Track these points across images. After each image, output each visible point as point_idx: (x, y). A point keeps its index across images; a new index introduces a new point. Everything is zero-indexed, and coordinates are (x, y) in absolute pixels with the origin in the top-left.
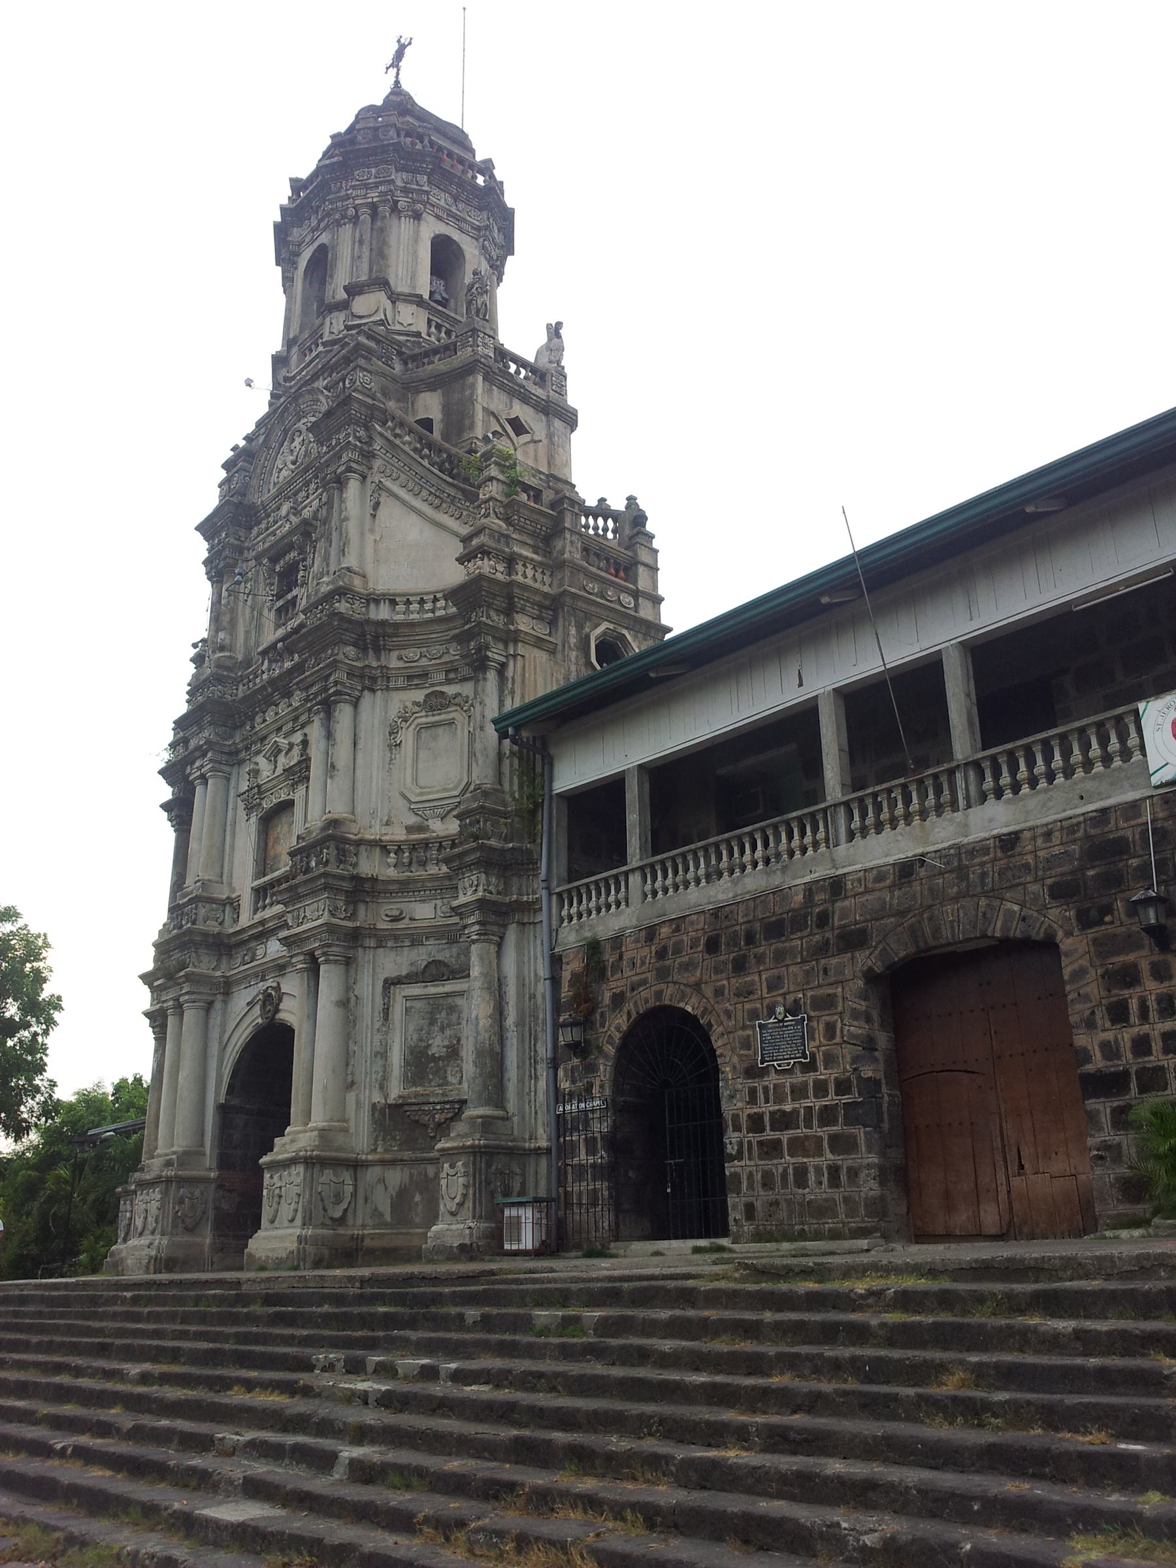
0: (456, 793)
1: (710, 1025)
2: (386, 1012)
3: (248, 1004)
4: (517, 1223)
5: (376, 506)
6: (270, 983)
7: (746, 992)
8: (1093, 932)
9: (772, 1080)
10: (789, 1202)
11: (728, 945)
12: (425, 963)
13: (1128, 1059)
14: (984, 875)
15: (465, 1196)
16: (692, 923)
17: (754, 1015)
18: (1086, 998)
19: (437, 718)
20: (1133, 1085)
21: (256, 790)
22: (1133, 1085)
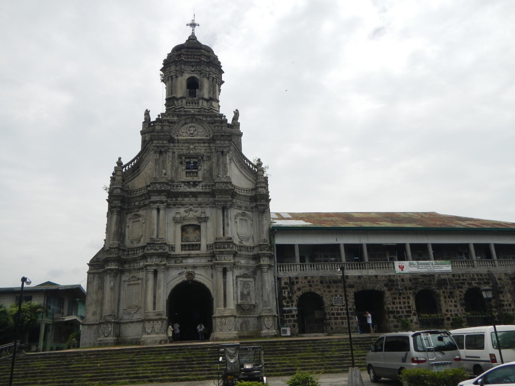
0: (248, 236)
1: (323, 296)
2: (237, 282)
3: (179, 274)
4: (285, 331)
5: (231, 162)
6: (190, 270)
7: (330, 292)
8: (390, 292)
9: (336, 307)
10: (340, 327)
11: (325, 283)
12: (243, 274)
13: (395, 309)
14: (373, 280)
15: (272, 325)
16: (316, 277)
17: (332, 296)
18: (389, 300)
19: (243, 218)
20: (396, 313)
21: (183, 218)
22: (396, 313)
